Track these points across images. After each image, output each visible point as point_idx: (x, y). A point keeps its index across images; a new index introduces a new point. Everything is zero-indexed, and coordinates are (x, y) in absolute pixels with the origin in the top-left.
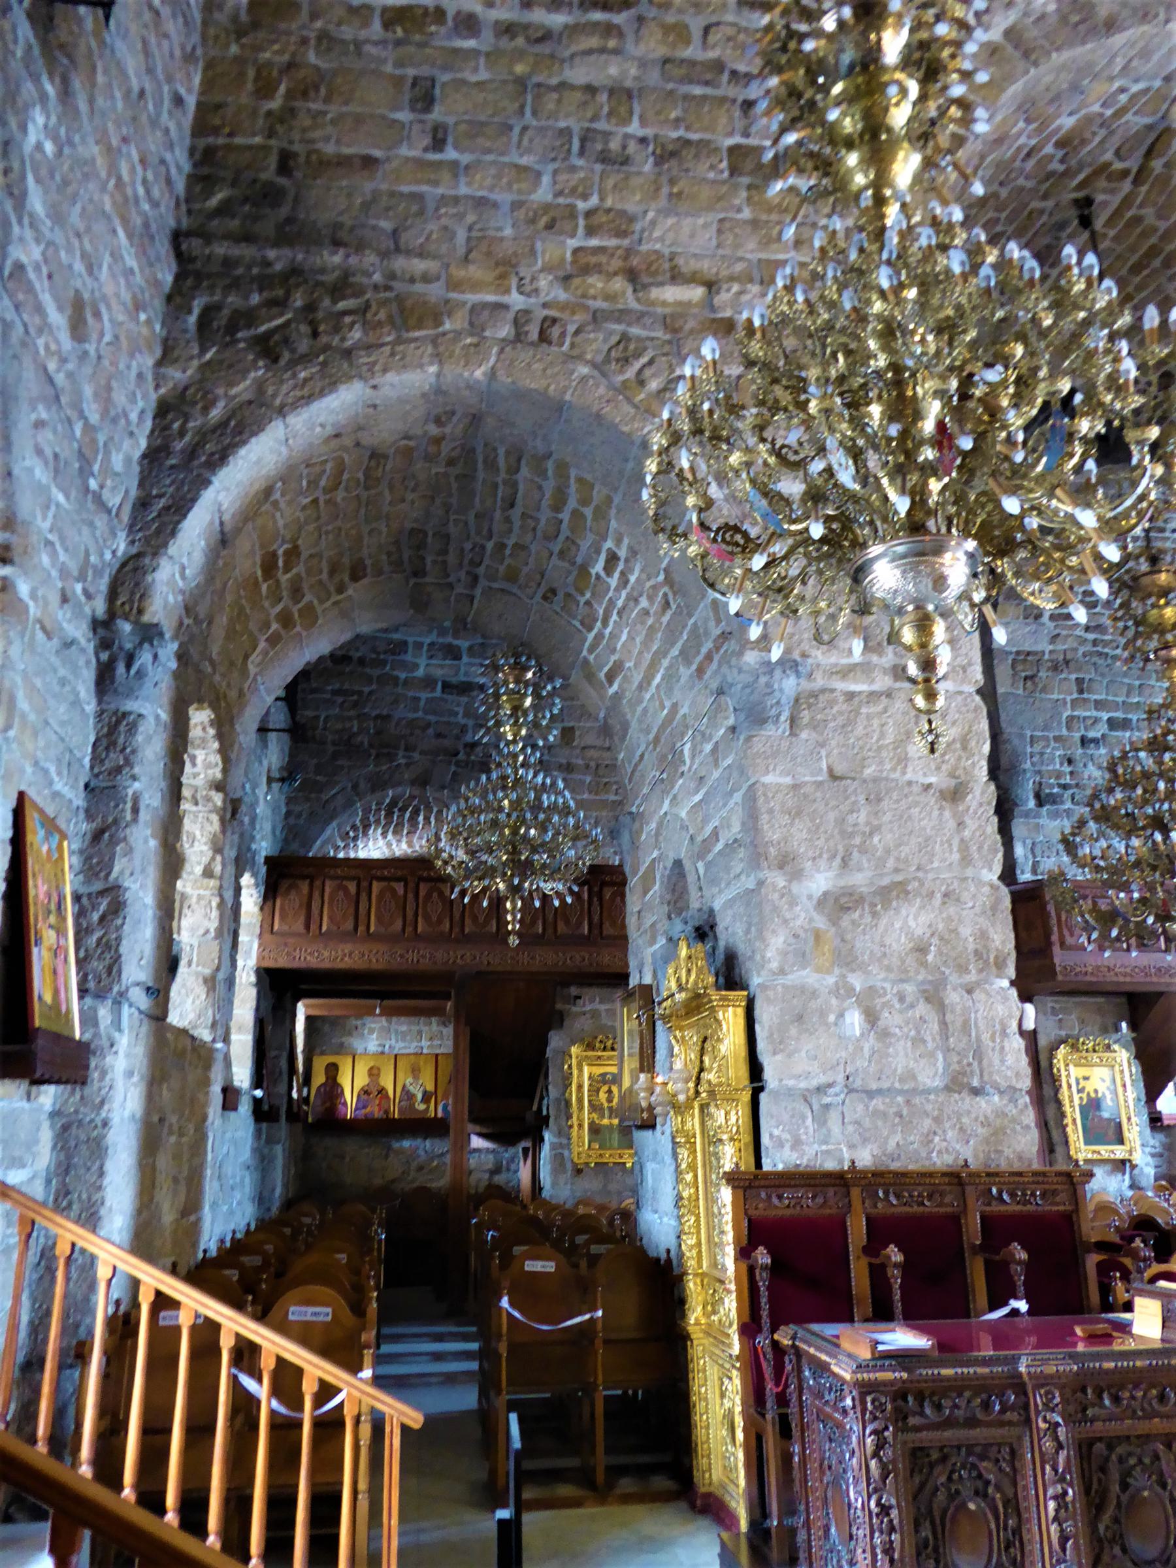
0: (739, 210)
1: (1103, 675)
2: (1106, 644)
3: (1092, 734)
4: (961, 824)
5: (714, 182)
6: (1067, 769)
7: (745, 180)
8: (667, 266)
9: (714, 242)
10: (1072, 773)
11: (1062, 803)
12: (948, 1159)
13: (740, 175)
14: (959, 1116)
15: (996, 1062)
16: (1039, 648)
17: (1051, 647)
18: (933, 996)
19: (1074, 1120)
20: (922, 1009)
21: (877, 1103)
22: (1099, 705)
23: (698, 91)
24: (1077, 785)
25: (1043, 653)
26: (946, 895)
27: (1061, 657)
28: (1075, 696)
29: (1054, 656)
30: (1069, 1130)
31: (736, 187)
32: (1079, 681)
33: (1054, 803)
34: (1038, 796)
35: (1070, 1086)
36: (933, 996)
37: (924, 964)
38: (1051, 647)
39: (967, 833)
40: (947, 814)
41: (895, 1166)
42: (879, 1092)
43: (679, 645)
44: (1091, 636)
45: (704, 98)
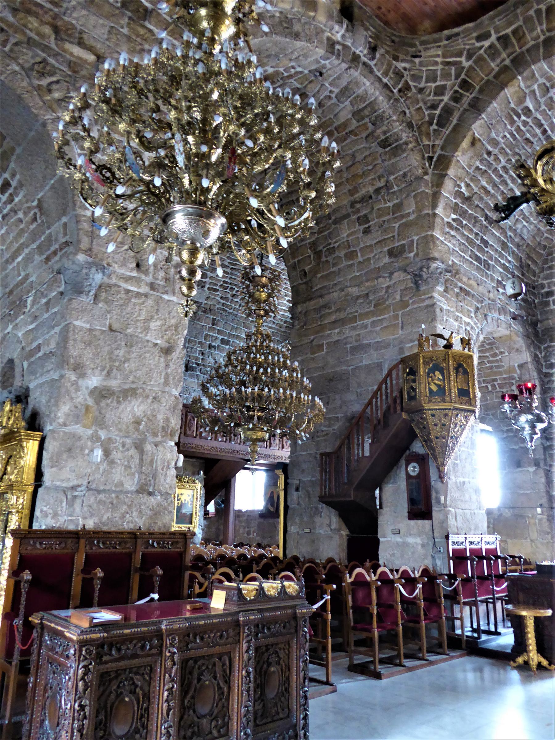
1: (223, 319)
2: (227, 306)
3: (214, 344)
4: (167, 366)
6: (201, 357)
8: (77, 35)
9: (106, 36)
10: (202, 359)
11: (196, 371)
12: (131, 526)
13: (127, 9)
14: (140, 505)
15: (162, 480)
18: (139, 447)
20: (133, 452)
21: (102, 496)
22: (219, 332)
24: (203, 365)
26: (154, 398)
27: (208, 308)
28: (211, 326)
29: (206, 306)
31: (123, 14)
32: (214, 320)
33: (193, 371)
36: (139, 447)
37: (137, 430)
39: (169, 371)
40: (162, 359)
41: (105, 528)
42: (104, 491)
43: (38, 243)
44: (222, 301)
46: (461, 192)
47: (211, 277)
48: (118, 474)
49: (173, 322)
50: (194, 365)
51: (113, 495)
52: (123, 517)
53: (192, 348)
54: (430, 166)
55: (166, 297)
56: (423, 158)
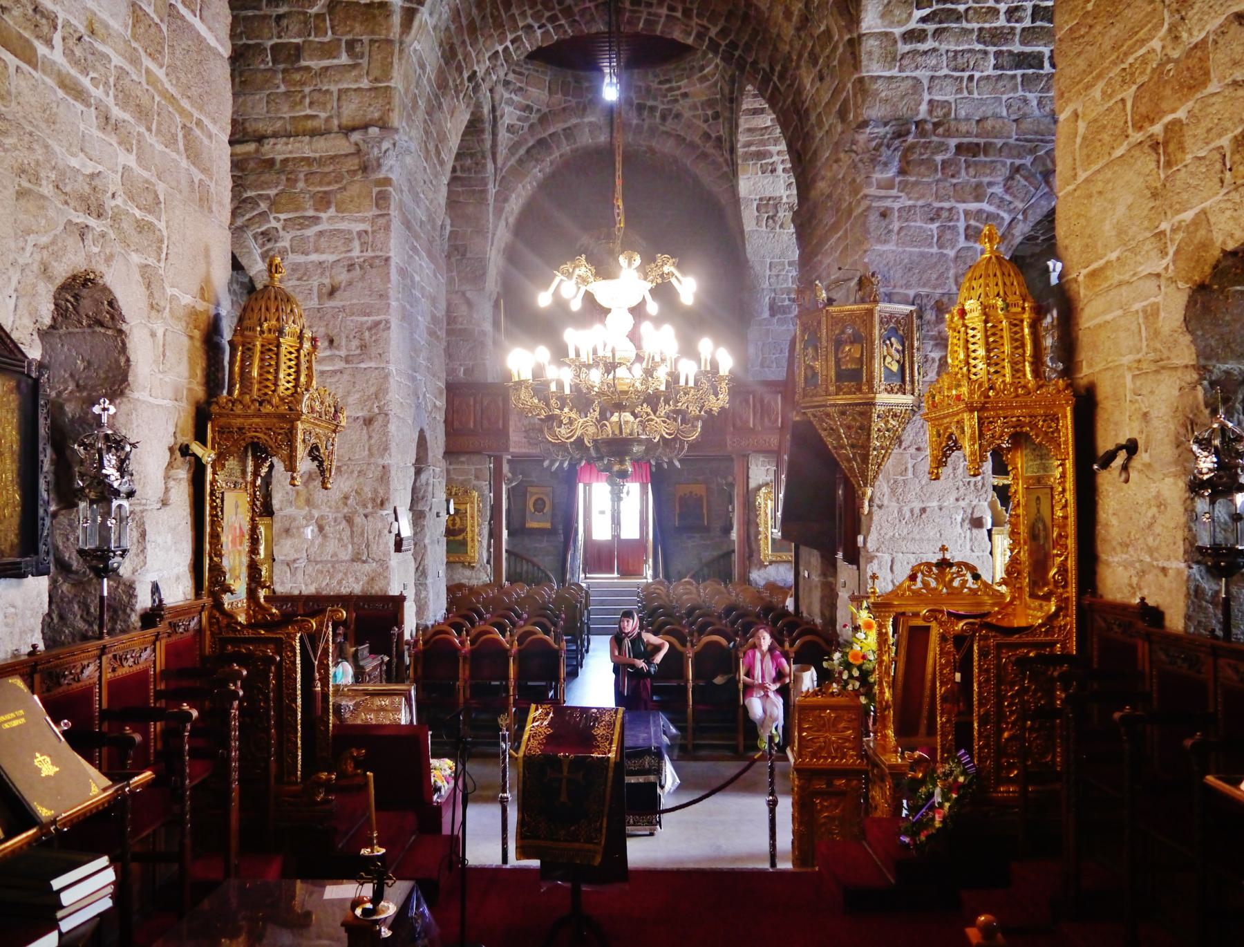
0: (278, 87)
4: (370, 437)
5: (265, 70)
7: (281, 66)
8: (241, 128)
9: (265, 109)
11: (790, 312)
13: (279, 63)
14: (355, 572)
15: (375, 548)
17: (788, 192)
18: (349, 520)
19: (766, 537)
20: (344, 524)
21: (319, 566)
23: (250, 13)
25: (781, 198)
26: (359, 472)
31: (275, 72)
33: (784, 313)
34: (771, 308)
35: (766, 514)
36: (349, 520)
37: (346, 504)
38: (788, 192)
39: (373, 441)
40: (365, 431)
41: (324, 593)
42: (321, 562)
45: (255, 16)
47: (779, 153)
48: (332, 546)
49: (373, 390)
50: (787, 303)
51: (329, 565)
52: (340, 582)
53: (778, 276)
55: (363, 365)
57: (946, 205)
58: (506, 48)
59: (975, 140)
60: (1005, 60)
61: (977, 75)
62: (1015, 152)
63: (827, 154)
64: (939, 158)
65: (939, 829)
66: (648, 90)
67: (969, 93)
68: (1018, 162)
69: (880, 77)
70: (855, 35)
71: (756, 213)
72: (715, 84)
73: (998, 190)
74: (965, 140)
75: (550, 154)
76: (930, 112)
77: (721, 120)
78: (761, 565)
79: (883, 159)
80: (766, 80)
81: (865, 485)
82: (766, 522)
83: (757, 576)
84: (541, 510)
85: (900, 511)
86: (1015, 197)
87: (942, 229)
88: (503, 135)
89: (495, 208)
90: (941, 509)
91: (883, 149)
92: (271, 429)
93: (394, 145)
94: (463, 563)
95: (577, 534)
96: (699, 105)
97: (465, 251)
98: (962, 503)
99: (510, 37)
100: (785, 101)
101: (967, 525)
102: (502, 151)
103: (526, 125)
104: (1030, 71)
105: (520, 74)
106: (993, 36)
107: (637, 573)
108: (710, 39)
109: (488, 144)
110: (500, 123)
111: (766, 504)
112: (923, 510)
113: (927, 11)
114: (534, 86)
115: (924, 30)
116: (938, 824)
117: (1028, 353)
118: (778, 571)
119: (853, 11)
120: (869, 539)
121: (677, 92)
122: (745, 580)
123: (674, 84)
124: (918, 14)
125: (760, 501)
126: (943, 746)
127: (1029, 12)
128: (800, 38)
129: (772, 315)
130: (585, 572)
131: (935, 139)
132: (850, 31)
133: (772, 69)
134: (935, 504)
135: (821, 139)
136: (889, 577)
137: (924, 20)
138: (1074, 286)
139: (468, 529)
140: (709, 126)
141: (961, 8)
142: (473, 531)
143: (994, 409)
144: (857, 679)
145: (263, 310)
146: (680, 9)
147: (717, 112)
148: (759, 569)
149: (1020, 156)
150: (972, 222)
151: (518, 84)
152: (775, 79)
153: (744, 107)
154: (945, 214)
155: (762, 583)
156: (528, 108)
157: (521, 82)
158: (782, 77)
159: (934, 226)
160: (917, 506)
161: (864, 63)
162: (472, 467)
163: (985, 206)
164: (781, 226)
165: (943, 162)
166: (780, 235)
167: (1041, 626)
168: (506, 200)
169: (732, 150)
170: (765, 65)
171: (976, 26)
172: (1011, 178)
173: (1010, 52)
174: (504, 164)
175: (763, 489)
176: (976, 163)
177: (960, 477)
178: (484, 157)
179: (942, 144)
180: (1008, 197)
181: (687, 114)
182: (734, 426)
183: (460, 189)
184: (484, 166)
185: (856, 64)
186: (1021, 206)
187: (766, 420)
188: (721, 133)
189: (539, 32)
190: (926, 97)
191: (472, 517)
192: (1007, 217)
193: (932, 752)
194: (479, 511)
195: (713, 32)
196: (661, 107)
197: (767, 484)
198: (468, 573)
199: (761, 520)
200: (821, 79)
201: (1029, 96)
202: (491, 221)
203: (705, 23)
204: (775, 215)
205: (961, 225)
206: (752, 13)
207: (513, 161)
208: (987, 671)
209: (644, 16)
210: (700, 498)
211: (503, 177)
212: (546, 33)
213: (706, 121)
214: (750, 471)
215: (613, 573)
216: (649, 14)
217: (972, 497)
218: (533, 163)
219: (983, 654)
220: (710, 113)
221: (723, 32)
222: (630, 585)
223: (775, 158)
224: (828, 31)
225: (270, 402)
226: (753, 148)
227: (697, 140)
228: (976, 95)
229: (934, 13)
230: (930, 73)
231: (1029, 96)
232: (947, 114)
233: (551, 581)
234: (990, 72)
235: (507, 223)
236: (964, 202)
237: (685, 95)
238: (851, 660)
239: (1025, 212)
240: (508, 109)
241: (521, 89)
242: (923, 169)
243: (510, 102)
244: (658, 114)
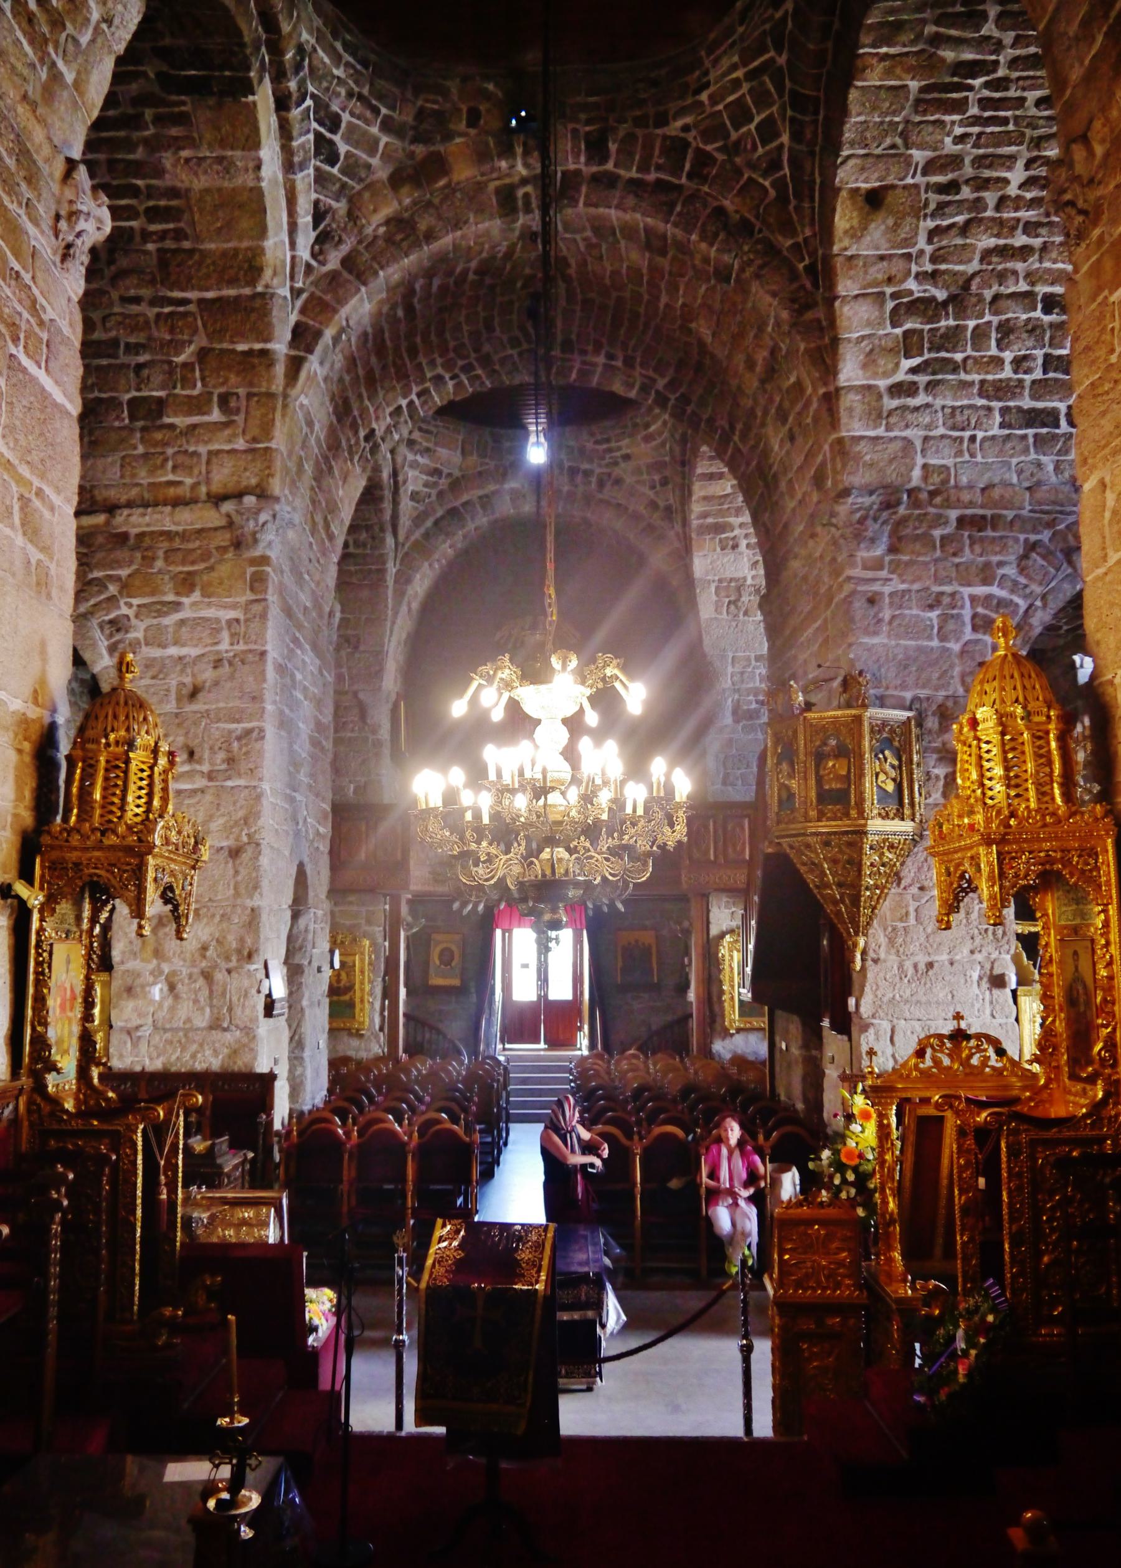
0: (135, 448)
4: (237, 872)
5: (120, 428)
7: (140, 424)
11: (758, 717)
12: (204, 1066)
13: (137, 420)
16: (740, 575)
17: (754, 572)
19: (732, 998)
20: (201, 982)
21: (168, 1035)
23: (104, 362)
25: (745, 579)
26: (222, 916)
30: (726, 1005)
31: (132, 430)
33: (751, 718)
34: (735, 712)
35: (732, 969)
36: (207, 976)
37: (204, 957)
39: (239, 878)
40: (230, 865)
41: (173, 1069)
42: (171, 1029)
45: (110, 365)
46: (918, 299)
47: (741, 525)
48: (185, 1009)
49: (241, 814)
51: (181, 1034)
52: (194, 1056)
53: (742, 673)
54: (816, 285)
55: (229, 783)
56: (794, 276)
57: (948, 589)
58: (411, 403)
59: (980, 512)
60: (1012, 418)
61: (980, 435)
62: (1029, 527)
63: (801, 528)
64: (937, 533)
65: (963, 1385)
66: (582, 451)
67: (972, 455)
68: (1033, 538)
69: (862, 438)
70: (832, 388)
71: (714, 598)
72: (663, 444)
73: (1011, 571)
74: (969, 512)
75: (463, 527)
76: (925, 478)
77: (670, 486)
78: (726, 1034)
79: (869, 534)
80: (726, 439)
81: (857, 934)
82: (732, 980)
83: (722, 1048)
84: (448, 963)
85: (901, 966)
86: (1030, 579)
87: (944, 618)
88: (407, 506)
89: (395, 591)
90: (952, 964)
91: (869, 522)
92: (114, 865)
93: (274, 516)
94: (349, 1030)
95: (493, 993)
96: (644, 469)
97: (358, 642)
98: (979, 957)
99: (415, 389)
100: (748, 464)
101: (985, 984)
102: (405, 522)
103: (434, 492)
104: (1044, 431)
105: (427, 432)
106: (998, 389)
107: (570, 1043)
108: (657, 392)
109: (387, 515)
110: (401, 491)
111: (732, 957)
112: (930, 965)
113: (915, 361)
114: (443, 447)
115: (915, 383)
116: (961, 1379)
117: (1057, 772)
118: (747, 1042)
119: (828, 361)
120: (863, 1002)
121: (618, 454)
122: (706, 1051)
123: (613, 445)
124: (907, 364)
125: (723, 951)
126: (965, 1273)
127: (1040, 361)
128: (765, 391)
129: (737, 721)
130: (503, 1041)
131: (932, 510)
132: (826, 384)
133: (732, 428)
134: (944, 957)
135: (794, 510)
136: (889, 1050)
137: (913, 370)
138: (1110, 690)
139: (357, 987)
140: (657, 493)
141: (959, 357)
142: (362, 990)
143: (1016, 841)
144: (852, 1184)
145: (110, 718)
146: (620, 355)
147: (666, 478)
148: (723, 1039)
149: (1035, 531)
150: (980, 610)
151: (425, 444)
152: (736, 438)
153: (699, 471)
154: (946, 600)
155: (728, 1056)
156: (436, 472)
157: (428, 441)
158: (744, 436)
159: (934, 615)
160: (922, 960)
161: (844, 420)
162: (363, 909)
163: (994, 590)
164: (746, 613)
165: (943, 538)
166: (744, 623)
167: (1085, 1116)
168: (409, 581)
169: (685, 522)
170: (723, 423)
171: (976, 377)
172: (1025, 556)
173: (1019, 409)
174: (407, 538)
175: (728, 938)
176: (982, 540)
177: (975, 923)
178: (382, 530)
179: (940, 516)
180: (1023, 580)
181: (629, 480)
182: (690, 858)
183: (352, 568)
184: (383, 540)
185: (835, 424)
186: (1038, 589)
187: (730, 850)
188: (671, 501)
189: (451, 384)
190: (920, 461)
191: (362, 972)
192: (1023, 604)
193: (950, 1280)
194: (370, 964)
195: (661, 383)
196: (598, 471)
197: (731, 931)
198: (355, 1042)
199: (725, 976)
200: (792, 438)
201: (1044, 459)
202: (390, 606)
203: (651, 373)
204: (738, 600)
205: (967, 613)
206: (708, 362)
207: (417, 535)
208: (1019, 1175)
209: (577, 365)
210: (650, 947)
211: (407, 554)
212: (459, 386)
213: (653, 487)
214: (711, 915)
215: (538, 1042)
216: (584, 363)
217: (990, 948)
218: (442, 537)
219: (1013, 1153)
220: (657, 477)
221: (672, 385)
222: (560, 1059)
223: (737, 532)
224: (799, 386)
225: (114, 832)
226: (710, 520)
227: (641, 509)
228: (979, 459)
229: (926, 363)
230: (922, 433)
231: (1044, 459)
232: (945, 481)
233: (460, 1053)
234: (995, 431)
235: (410, 610)
236: (969, 585)
237: (627, 457)
238: (844, 1160)
239: (1044, 597)
240: (411, 474)
241: (428, 450)
242: (918, 546)
243: (414, 465)
244: (594, 480)
